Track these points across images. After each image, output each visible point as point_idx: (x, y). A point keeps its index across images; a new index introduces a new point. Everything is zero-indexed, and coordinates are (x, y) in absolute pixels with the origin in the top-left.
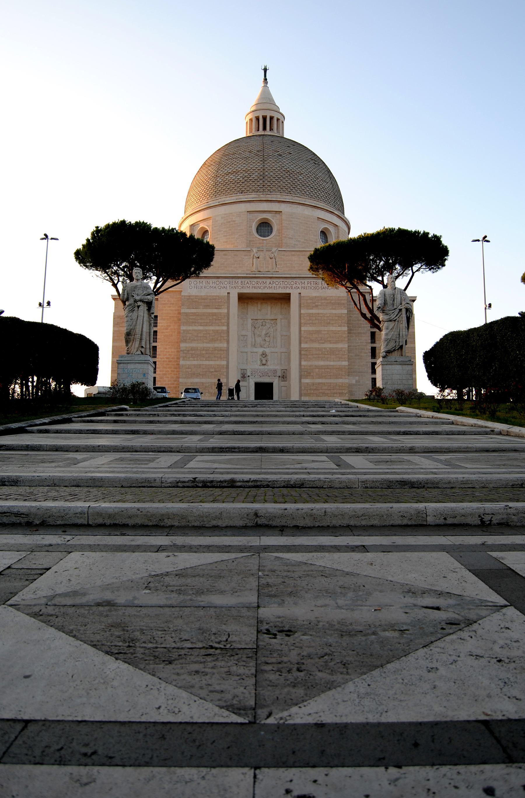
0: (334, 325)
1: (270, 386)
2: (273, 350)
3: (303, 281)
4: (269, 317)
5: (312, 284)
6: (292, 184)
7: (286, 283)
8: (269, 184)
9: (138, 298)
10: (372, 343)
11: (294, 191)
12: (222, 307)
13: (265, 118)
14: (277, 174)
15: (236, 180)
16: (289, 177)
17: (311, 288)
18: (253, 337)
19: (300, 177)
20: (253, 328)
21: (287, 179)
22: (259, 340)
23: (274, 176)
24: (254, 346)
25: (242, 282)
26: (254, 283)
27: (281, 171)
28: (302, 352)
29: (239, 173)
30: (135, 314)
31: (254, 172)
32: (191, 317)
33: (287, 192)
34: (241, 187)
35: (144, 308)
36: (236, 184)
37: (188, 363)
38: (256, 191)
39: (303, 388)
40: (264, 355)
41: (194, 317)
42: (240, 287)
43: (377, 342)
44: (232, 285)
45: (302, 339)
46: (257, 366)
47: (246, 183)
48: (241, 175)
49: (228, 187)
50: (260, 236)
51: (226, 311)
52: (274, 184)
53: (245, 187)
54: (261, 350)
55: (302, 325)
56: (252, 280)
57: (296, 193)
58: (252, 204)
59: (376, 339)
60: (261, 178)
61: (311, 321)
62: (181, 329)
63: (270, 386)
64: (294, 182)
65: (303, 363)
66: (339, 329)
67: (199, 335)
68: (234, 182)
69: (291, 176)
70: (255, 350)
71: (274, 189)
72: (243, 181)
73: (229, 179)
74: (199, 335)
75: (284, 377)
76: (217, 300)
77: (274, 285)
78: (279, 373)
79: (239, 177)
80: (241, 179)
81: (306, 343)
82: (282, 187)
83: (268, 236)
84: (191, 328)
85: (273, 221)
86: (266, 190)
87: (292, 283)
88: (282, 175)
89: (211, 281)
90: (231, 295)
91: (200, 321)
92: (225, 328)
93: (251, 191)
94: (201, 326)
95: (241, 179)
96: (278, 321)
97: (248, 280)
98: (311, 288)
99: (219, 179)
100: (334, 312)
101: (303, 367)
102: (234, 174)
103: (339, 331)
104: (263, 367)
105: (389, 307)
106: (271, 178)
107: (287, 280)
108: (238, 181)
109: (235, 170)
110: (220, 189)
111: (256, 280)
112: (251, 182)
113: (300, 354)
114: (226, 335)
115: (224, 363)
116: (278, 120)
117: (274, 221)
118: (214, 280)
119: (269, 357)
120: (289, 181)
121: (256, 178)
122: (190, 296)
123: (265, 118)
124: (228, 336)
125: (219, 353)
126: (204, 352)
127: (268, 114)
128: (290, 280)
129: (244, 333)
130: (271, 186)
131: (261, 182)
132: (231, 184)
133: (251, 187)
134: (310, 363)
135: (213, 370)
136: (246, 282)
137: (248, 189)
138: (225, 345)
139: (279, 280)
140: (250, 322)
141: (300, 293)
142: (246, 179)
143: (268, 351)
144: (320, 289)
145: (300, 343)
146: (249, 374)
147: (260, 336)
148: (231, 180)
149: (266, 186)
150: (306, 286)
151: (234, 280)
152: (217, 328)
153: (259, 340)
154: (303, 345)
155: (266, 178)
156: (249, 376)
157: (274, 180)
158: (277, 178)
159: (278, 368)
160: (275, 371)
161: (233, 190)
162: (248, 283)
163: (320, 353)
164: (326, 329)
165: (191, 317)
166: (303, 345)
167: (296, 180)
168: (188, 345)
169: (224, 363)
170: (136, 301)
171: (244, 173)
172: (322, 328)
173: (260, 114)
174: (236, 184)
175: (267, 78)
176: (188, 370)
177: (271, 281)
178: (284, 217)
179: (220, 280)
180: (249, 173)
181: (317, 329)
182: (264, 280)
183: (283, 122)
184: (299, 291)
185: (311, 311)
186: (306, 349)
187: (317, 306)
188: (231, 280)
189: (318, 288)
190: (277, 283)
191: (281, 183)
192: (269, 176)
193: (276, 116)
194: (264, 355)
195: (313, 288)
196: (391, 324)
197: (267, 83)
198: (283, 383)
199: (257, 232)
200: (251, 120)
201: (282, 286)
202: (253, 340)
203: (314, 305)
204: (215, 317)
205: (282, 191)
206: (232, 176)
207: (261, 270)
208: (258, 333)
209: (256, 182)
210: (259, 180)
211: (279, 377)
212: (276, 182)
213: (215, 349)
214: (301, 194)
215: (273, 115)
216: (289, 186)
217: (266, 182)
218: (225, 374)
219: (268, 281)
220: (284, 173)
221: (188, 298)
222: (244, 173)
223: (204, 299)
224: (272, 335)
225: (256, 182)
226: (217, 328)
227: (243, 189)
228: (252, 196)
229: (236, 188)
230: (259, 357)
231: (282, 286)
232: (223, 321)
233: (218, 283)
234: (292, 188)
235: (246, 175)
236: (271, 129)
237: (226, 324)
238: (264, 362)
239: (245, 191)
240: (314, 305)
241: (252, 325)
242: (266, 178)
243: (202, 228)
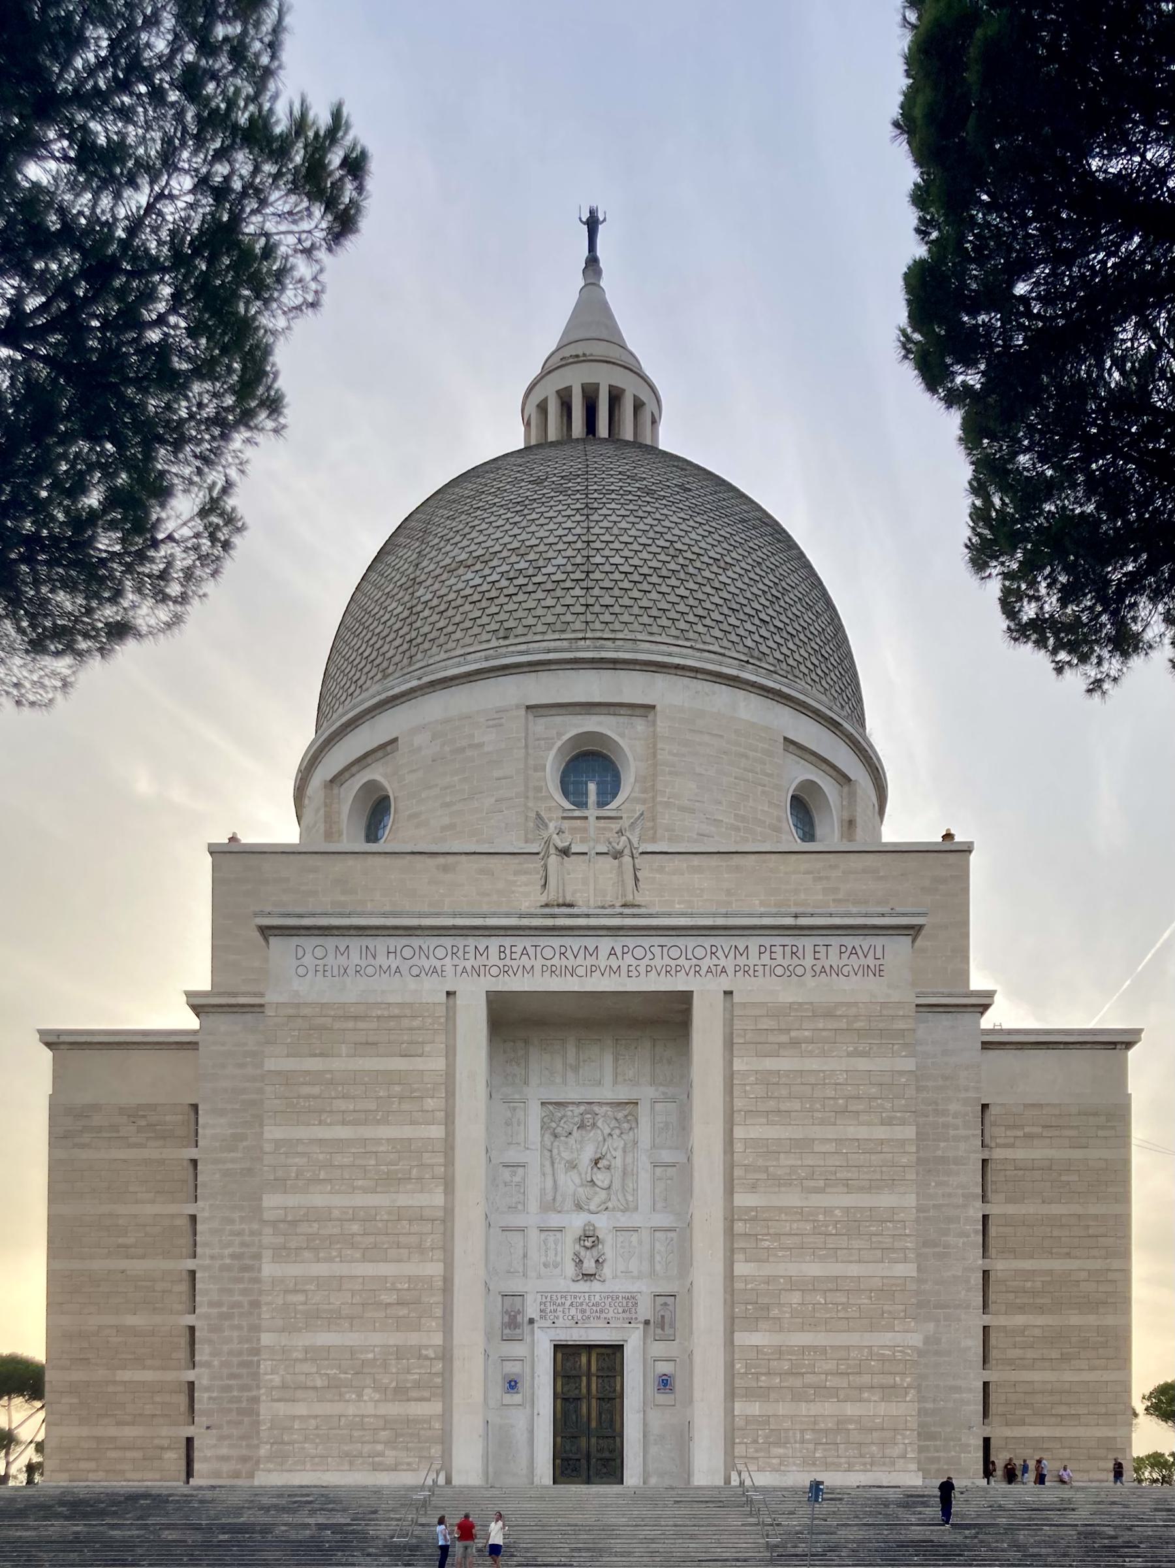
0: (864, 1117)
2: (624, 1220)
3: (741, 943)
4: (607, 1093)
5: (778, 955)
6: (691, 602)
7: (675, 953)
8: (608, 600)
11: (700, 628)
12: (427, 1048)
14: (636, 561)
15: (485, 587)
16: (682, 575)
17: (772, 971)
18: (548, 1169)
19: (723, 578)
20: (548, 1137)
21: (673, 582)
22: (569, 1183)
23: (626, 568)
24: (550, 1205)
25: (501, 950)
26: (548, 953)
27: (654, 549)
28: (739, 1227)
29: (495, 563)
31: (551, 554)
32: (306, 1090)
33: (673, 632)
34: (503, 616)
36: (484, 604)
37: (293, 1270)
38: (558, 626)
40: (589, 1239)
41: (316, 1090)
42: (494, 971)
44: (462, 964)
45: (738, 1172)
46: (563, 1280)
47: (521, 597)
48: (505, 568)
49: (457, 619)
51: (440, 1064)
52: (626, 601)
53: (520, 614)
54: (577, 1222)
55: (738, 1118)
56: (542, 941)
57: (708, 639)
58: (544, 677)
60: (578, 575)
61: (772, 1104)
62: (267, 1136)
64: (700, 596)
65: (742, 1268)
66: (881, 1133)
67: (338, 1160)
68: (476, 597)
69: (691, 570)
70: (554, 1220)
71: (626, 618)
72: (512, 590)
73: (461, 585)
74: (338, 1160)
76: (406, 1023)
77: (628, 957)
79: (495, 577)
80: (504, 583)
81: (753, 1188)
82: (654, 612)
84: (302, 1133)
86: (598, 625)
87: (699, 952)
88: (654, 564)
89: (380, 944)
90: (460, 1001)
91: (341, 1105)
92: (436, 1132)
93: (540, 628)
94: (344, 1123)
95: (504, 583)
96: (643, 1111)
97: (527, 942)
98: (772, 971)
99: (421, 591)
100: (862, 1064)
101: (739, 1285)
102: (478, 566)
103: (882, 1142)
104: (583, 1286)
106: (617, 576)
108: (494, 593)
109: (480, 552)
110: (426, 629)
112: (540, 595)
114: (440, 1159)
115: (434, 1269)
119: (608, 1249)
120: (682, 591)
121: (559, 576)
122: (298, 1005)
124: (449, 1162)
125: (415, 1228)
126: (355, 1228)
127: (606, 378)
128: (691, 942)
129: (513, 1156)
130: (617, 609)
131: (578, 592)
132: (468, 607)
133: (539, 612)
134: (768, 1270)
135: (392, 1298)
136: (519, 949)
137: (531, 621)
138: (438, 1199)
139: (646, 942)
140: (535, 1114)
141: (728, 993)
142: (521, 581)
144: (809, 973)
145: (729, 1191)
146: (532, 1311)
147: (572, 1166)
148: (468, 591)
149: (597, 609)
150: (751, 962)
152: (407, 1132)
153: (569, 1183)
154: (742, 1199)
155: (597, 575)
156: (531, 1321)
157: (626, 585)
158: (636, 577)
159: (644, 1288)
160: (631, 1300)
161: (476, 630)
162: (524, 951)
163: (809, 1227)
164: (830, 1132)
165: (306, 1090)
166: (742, 1199)
167: (708, 589)
168: (292, 1200)
169: (434, 1269)
171: (514, 559)
172: (817, 1132)
173: (575, 379)
174: (484, 604)
175: (600, 253)
176: (293, 1298)
177: (618, 943)
178: (662, 726)
179: (416, 942)
180: (532, 556)
181: (797, 1133)
184: (725, 983)
185: (770, 1064)
186: (755, 1215)
187: (795, 1043)
189: (799, 971)
190: (639, 952)
191: (654, 595)
192: (607, 568)
194: (589, 1239)
195: (779, 971)
197: (598, 273)
201: (658, 963)
202: (549, 1184)
203: (784, 1038)
204: (397, 1088)
205: (655, 629)
206: (470, 575)
208: (566, 1155)
209: (559, 593)
210: (568, 584)
211: (647, 1323)
212: (636, 594)
213: (400, 1214)
214: (725, 643)
216: (682, 608)
217: (596, 592)
218: (438, 1312)
220: (663, 557)
221: (291, 1011)
222: (514, 559)
223: (356, 1018)
224: (618, 1162)
225: (559, 593)
226: (407, 1132)
227: (511, 624)
229: (485, 620)
230: (569, 1246)
231: (658, 963)
232: (430, 1103)
233: (407, 952)
234: (691, 618)
235: (523, 565)
237: (440, 1115)
238: (589, 1266)
239: (520, 630)
240: (784, 1038)
242: (597, 575)
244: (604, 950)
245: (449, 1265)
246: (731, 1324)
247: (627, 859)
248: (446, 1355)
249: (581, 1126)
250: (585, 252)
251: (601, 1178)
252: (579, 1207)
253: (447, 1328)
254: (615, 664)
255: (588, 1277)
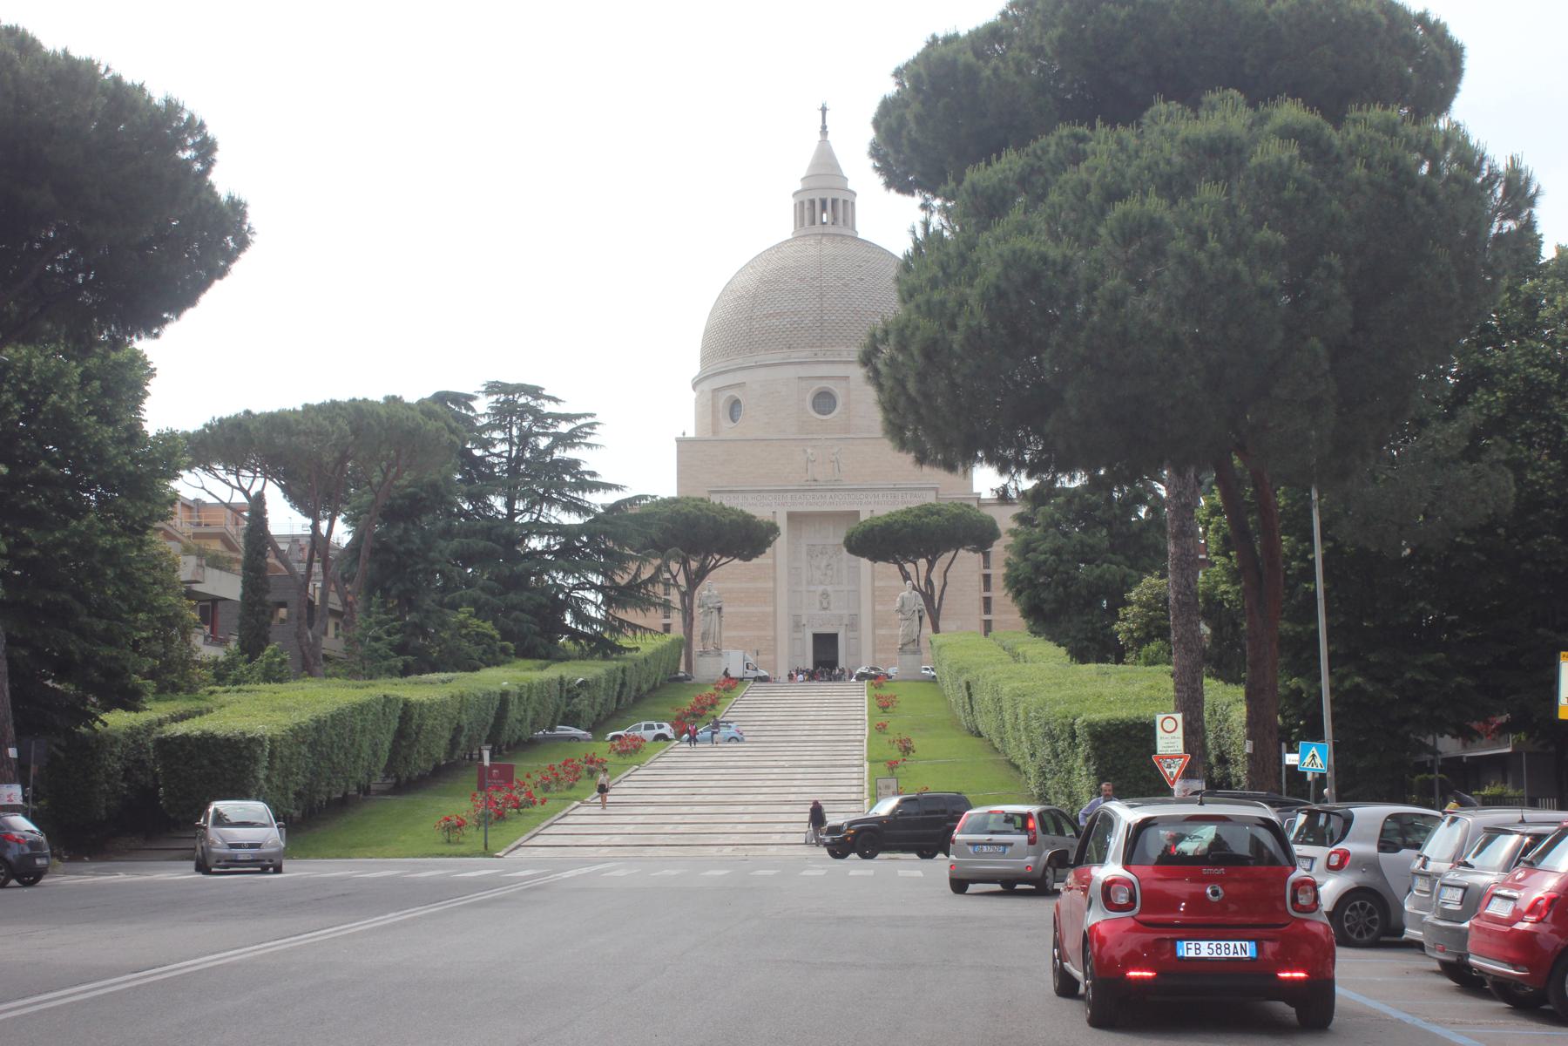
1: (833, 638)
8: (829, 334)
9: (711, 605)
10: (985, 568)
13: (824, 202)
28: (877, 593)
30: (709, 618)
35: (715, 613)
39: (877, 641)
40: (825, 595)
43: (992, 566)
50: (819, 413)
52: (837, 334)
54: (821, 589)
59: (991, 562)
63: (833, 638)
65: (878, 607)
70: (812, 588)
71: (838, 340)
75: (853, 624)
78: (846, 621)
83: (830, 412)
85: (837, 391)
89: (749, 496)
90: (777, 515)
105: (907, 608)
107: (855, 493)
111: (811, 494)
113: (873, 594)
115: (770, 609)
116: (845, 202)
117: (838, 390)
118: (756, 495)
123: (824, 202)
128: (859, 493)
138: (771, 584)
143: (829, 589)
146: (804, 622)
147: (818, 568)
151: (781, 494)
154: (877, 584)
158: (841, 324)
166: (877, 584)
170: (709, 608)
173: (817, 197)
177: (833, 494)
179: (762, 494)
182: (823, 494)
183: (853, 204)
188: (777, 494)
193: (841, 196)
194: (825, 595)
196: (907, 623)
198: (851, 634)
199: (814, 407)
200: (802, 203)
207: (818, 478)
215: (835, 197)
219: (828, 494)
228: (805, 354)
236: (835, 221)
238: (825, 605)
241: (808, 554)
243: (731, 396)
244: (828, 497)
245: (775, 607)
246: (874, 627)
247: (836, 465)
248: (775, 639)
249: (821, 553)
250: (821, 124)
251: (829, 572)
252: (821, 583)
253: (775, 629)
254: (833, 362)
255: (825, 609)
